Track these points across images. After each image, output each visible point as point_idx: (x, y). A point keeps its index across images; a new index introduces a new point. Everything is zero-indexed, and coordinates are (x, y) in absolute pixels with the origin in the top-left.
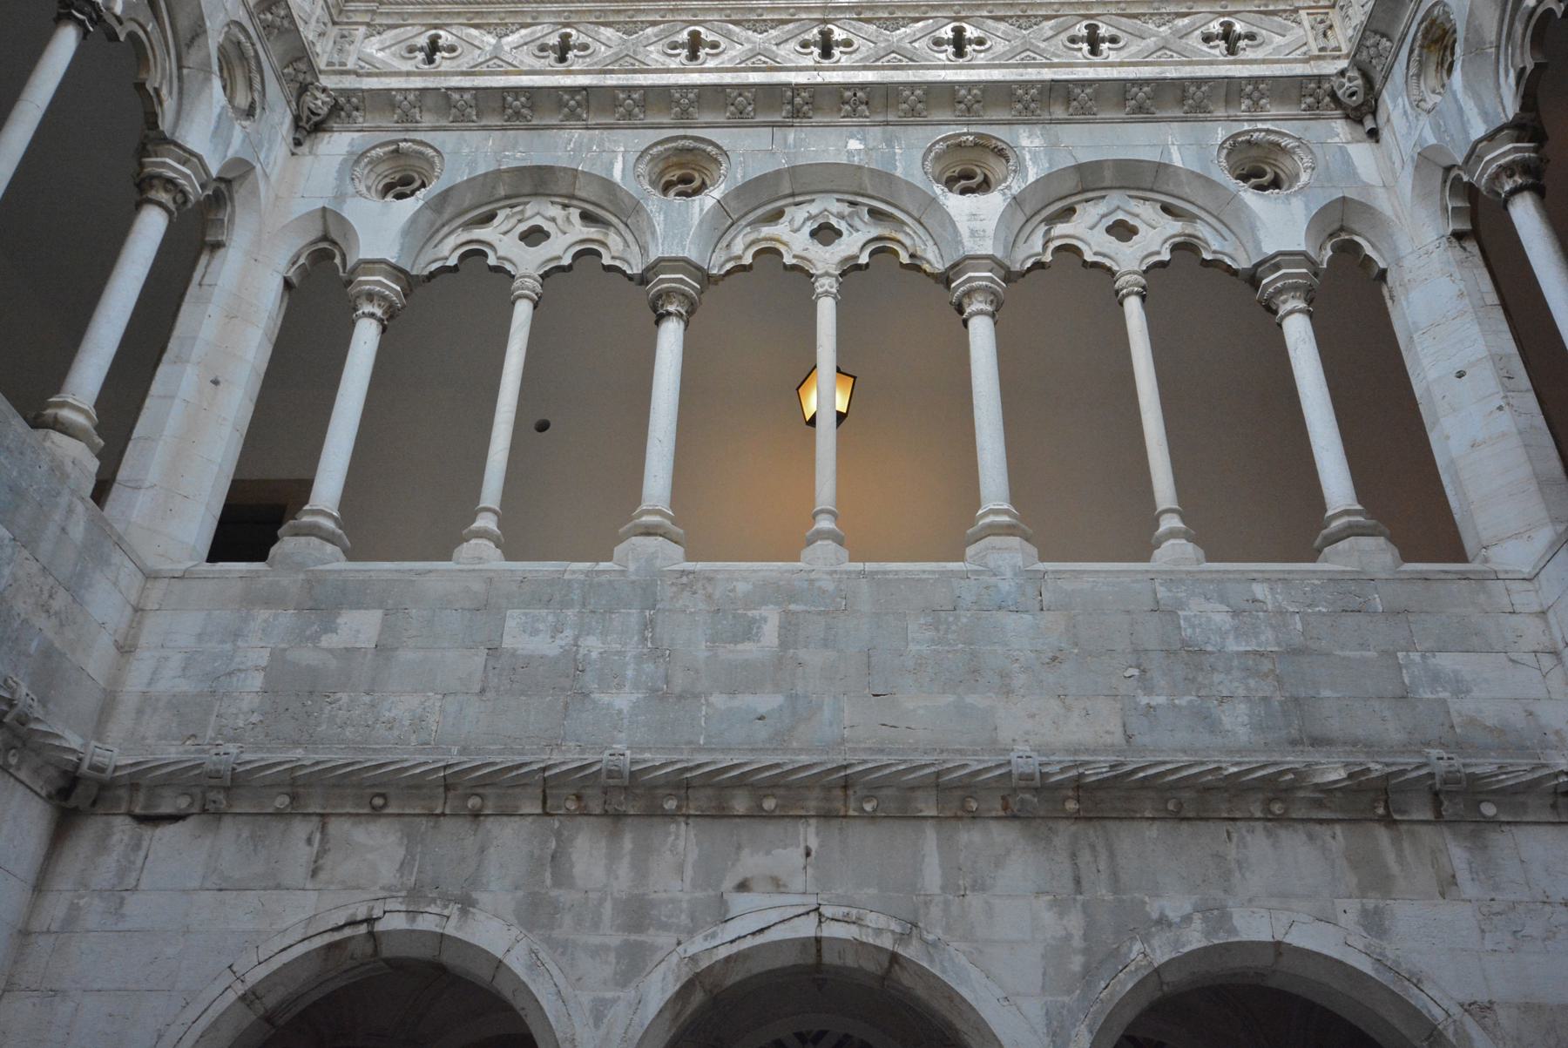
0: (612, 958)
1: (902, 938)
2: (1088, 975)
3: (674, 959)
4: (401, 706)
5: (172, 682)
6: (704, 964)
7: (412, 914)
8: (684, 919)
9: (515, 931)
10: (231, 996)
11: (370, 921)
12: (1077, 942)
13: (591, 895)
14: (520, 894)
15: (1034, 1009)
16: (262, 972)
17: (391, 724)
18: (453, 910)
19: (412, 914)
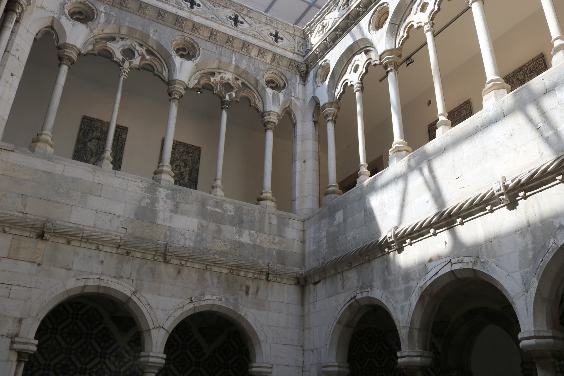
0: (403, 293)
1: (475, 263)
2: (535, 257)
3: (417, 289)
4: (351, 235)
5: (313, 247)
6: (424, 288)
7: (362, 293)
8: (418, 276)
9: (382, 291)
10: (335, 323)
11: (355, 297)
12: (530, 246)
13: (396, 276)
14: (381, 280)
15: (517, 276)
16: (339, 316)
17: (350, 241)
18: (369, 289)
19: (362, 293)
